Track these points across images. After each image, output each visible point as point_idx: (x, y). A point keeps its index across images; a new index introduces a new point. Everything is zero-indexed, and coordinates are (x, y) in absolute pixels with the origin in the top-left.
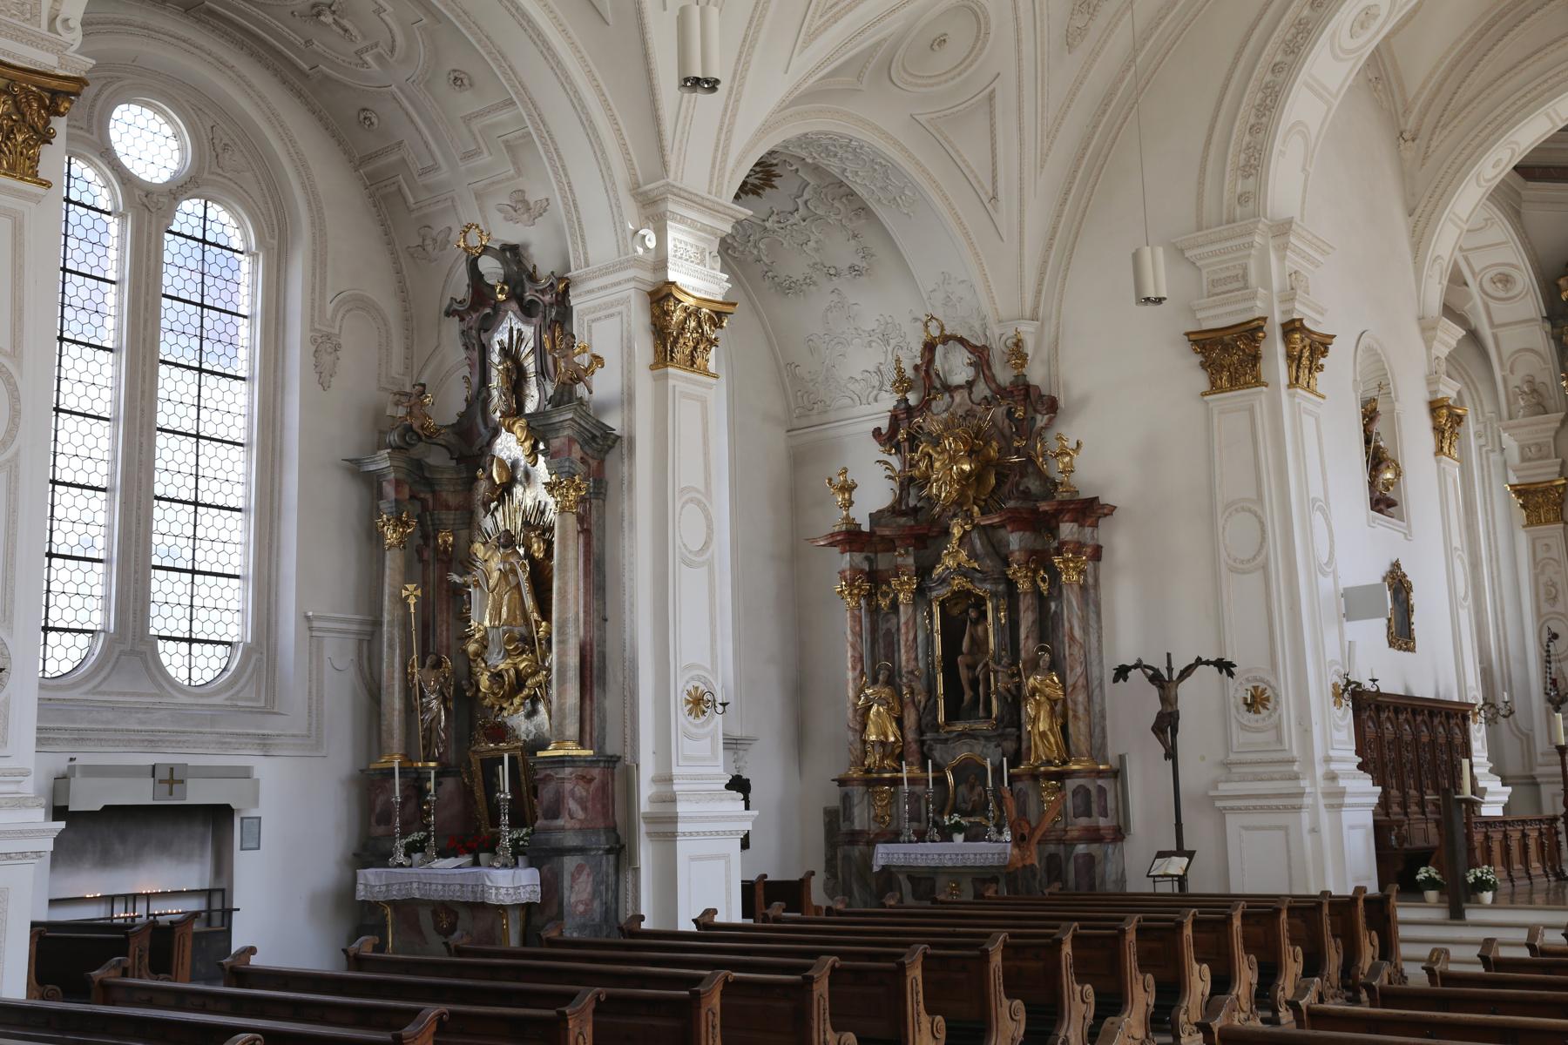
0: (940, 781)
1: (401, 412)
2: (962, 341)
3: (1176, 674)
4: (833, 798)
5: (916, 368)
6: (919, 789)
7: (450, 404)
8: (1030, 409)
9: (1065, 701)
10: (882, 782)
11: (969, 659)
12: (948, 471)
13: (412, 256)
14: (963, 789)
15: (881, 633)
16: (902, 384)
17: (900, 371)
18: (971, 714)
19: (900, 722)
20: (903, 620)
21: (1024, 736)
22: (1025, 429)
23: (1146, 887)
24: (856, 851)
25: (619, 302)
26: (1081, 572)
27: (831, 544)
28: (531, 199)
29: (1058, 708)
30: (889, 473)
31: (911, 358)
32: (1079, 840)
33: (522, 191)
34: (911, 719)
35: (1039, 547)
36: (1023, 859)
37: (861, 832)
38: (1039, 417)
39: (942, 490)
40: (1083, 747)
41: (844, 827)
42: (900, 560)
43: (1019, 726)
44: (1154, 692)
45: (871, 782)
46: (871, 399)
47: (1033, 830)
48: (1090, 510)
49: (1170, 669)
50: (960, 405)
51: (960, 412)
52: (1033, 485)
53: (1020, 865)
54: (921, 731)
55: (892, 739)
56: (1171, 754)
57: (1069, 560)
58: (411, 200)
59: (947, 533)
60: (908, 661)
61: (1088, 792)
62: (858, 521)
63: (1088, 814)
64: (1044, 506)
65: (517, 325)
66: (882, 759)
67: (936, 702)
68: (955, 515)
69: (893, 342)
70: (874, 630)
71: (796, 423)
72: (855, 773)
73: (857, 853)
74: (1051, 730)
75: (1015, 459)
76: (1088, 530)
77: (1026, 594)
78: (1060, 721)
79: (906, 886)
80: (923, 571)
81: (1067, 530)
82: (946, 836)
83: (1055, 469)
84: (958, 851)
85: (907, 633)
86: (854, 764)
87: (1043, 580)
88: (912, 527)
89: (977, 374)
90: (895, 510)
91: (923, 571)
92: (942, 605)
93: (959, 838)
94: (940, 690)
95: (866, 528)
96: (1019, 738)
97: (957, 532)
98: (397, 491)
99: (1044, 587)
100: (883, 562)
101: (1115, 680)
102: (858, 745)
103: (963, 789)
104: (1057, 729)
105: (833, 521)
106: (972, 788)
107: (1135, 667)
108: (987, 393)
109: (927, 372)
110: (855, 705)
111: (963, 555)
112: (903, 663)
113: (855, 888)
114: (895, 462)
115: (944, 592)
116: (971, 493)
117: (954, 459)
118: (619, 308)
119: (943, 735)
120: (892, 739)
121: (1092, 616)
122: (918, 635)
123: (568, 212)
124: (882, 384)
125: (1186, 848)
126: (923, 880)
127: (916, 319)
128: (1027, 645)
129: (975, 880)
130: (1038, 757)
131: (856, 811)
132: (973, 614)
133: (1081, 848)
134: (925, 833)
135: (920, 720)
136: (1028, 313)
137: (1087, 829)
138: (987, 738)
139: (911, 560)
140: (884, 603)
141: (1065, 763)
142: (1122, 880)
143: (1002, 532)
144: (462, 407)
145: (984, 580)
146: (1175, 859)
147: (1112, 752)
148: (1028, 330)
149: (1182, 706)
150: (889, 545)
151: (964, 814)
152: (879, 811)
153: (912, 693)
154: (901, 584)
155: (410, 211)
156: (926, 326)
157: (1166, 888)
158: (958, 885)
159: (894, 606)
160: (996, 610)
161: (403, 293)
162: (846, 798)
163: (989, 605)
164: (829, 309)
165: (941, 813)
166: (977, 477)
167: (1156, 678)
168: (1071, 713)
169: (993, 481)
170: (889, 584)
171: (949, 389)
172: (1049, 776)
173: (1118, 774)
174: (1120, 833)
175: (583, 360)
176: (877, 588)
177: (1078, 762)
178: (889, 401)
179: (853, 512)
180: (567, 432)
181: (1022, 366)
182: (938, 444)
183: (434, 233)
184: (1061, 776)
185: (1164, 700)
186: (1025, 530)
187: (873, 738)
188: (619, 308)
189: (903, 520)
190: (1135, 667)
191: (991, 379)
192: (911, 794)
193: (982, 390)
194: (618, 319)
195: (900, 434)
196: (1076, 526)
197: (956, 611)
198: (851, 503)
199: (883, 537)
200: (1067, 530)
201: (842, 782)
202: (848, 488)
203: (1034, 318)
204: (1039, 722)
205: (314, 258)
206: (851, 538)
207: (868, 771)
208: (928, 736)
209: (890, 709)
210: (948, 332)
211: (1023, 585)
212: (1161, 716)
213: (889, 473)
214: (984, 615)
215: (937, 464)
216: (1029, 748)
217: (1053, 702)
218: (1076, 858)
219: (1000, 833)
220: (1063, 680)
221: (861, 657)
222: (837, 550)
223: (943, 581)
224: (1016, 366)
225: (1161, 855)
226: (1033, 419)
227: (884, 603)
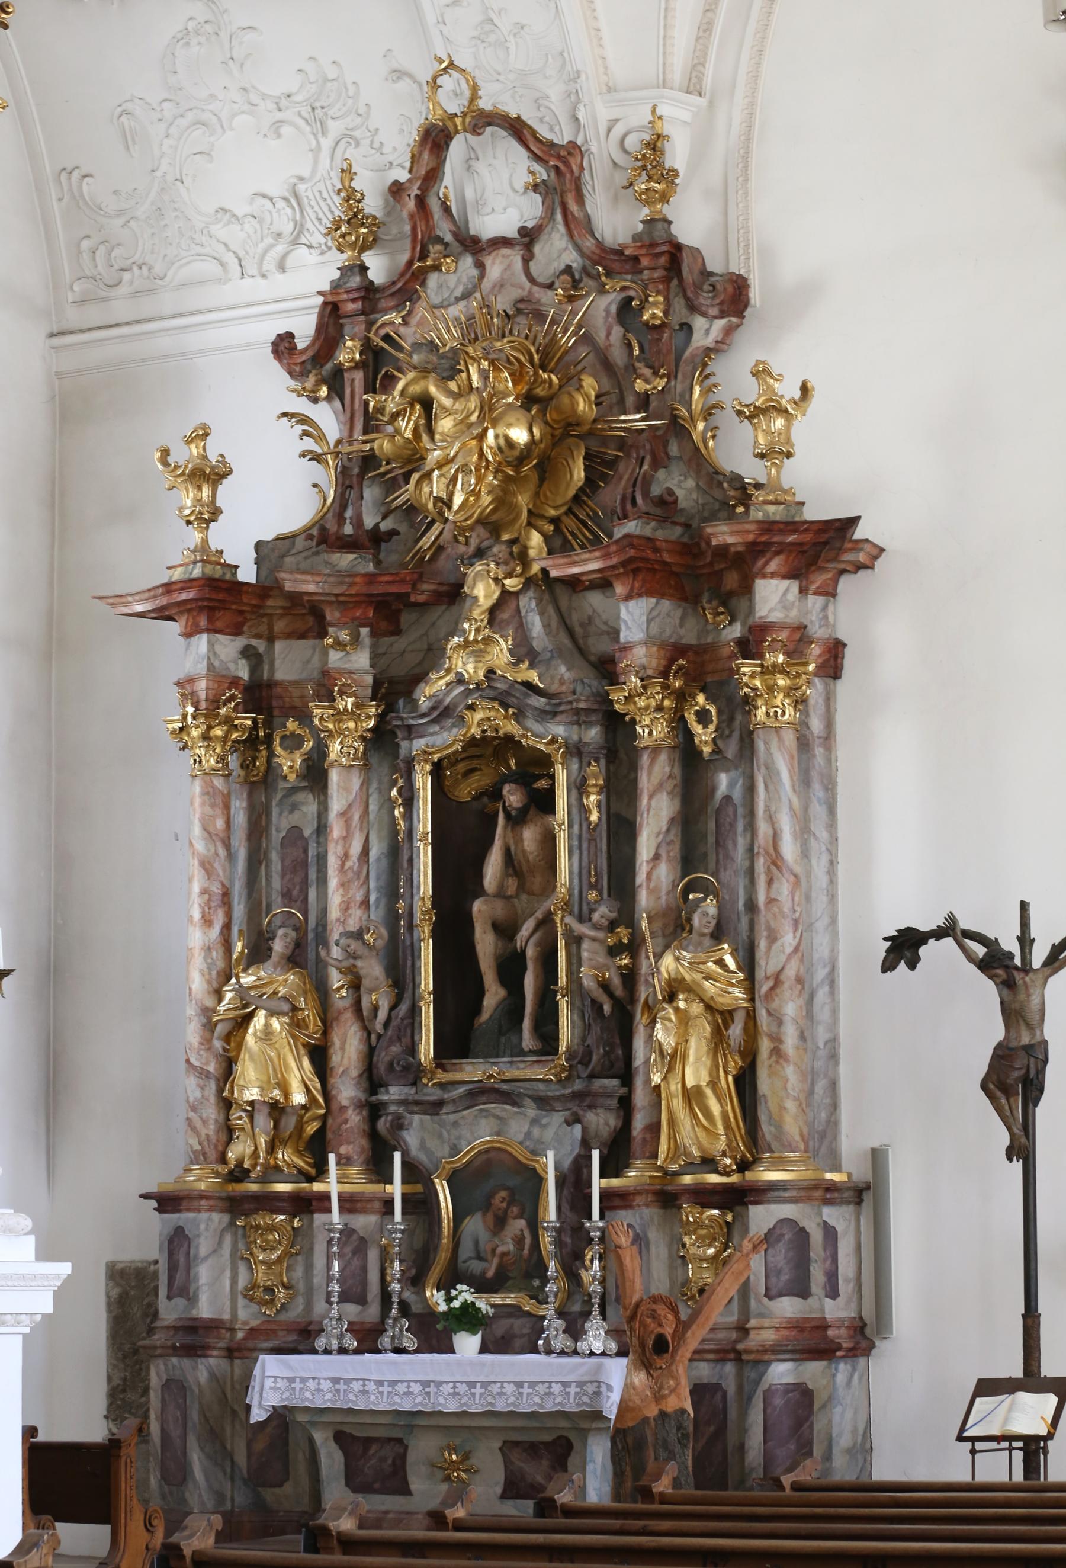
0: (420, 1205)
2: (517, 129)
3: (1038, 958)
4: (143, 1238)
5: (396, 190)
6: (365, 1222)
8: (679, 304)
9: (751, 1016)
10: (268, 1202)
11: (499, 909)
12: (467, 444)
14: (475, 1225)
15: (276, 837)
16: (355, 228)
17: (351, 197)
18: (503, 1037)
19: (319, 1056)
20: (336, 804)
21: (640, 1098)
22: (664, 349)
23: (953, 1467)
24: (200, 1373)
26: (800, 702)
27: (163, 614)
29: (736, 1031)
30: (309, 444)
31: (386, 156)
32: (777, 1351)
34: (348, 1049)
35: (689, 637)
36: (658, 1398)
37: (213, 1326)
38: (699, 323)
39: (455, 486)
40: (792, 1127)
41: (170, 1311)
42: (335, 657)
43: (627, 1076)
44: (986, 992)
45: (242, 1201)
46: (270, 263)
47: (683, 1327)
48: (827, 549)
49: (1025, 941)
50: (500, 285)
51: (503, 303)
52: (680, 484)
53: (652, 1412)
54: (372, 1081)
55: (299, 1098)
56: (1021, 1149)
57: (776, 669)
59: (454, 594)
60: (346, 908)
61: (802, 1235)
62: (229, 558)
63: (803, 1291)
64: (724, 534)
66: (271, 1149)
67: (414, 1011)
68: (480, 554)
69: (335, 128)
70: (258, 829)
71: (73, 317)
72: (201, 1179)
73: (203, 1376)
74: (714, 1084)
75: (635, 420)
76: (815, 602)
77: (656, 750)
78: (735, 1063)
79: (331, 1460)
80: (392, 690)
81: (774, 597)
82: (434, 1334)
83: (736, 451)
84: (465, 1375)
85: (346, 838)
86: (198, 1157)
87: (703, 717)
88: (375, 571)
89: (549, 214)
90: (323, 536)
91: (392, 690)
92: (437, 771)
93: (468, 1343)
94: (427, 981)
95: (247, 574)
96: (626, 1105)
97: (483, 592)
99: (704, 736)
100: (290, 661)
101: (888, 966)
102: (211, 1112)
103: (475, 1225)
104: (727, 1082)
105: (168, 551)
106: (500, 1223)
107: (939, 934)
108: (572, 258)
109: (421, 202)
110: (207, 1012)
111: (501, 653)
112: (334, 912)
113: (196, 1460)
114: (328, 418)
115: (445, 740)
116: (523, 500)
117: (489, 412)
119: (433, 1094)
120: (299, 1098)
121: (818, 811)
122: (363, 839)
124: (300, 229)
125: (1050, 1367)
126: (376, 1448)
127: (399, 74)
128: (655, 875)
129: (508, 1447)
130: (676, 1151)
131: (204, 1273)
132: (513, 797)
133: (781, 1372)
134: (379, 1330)
135: (370, 1053)
136: (677, 75)
137: (798, 1326)
138: (543, 1103)
139: (362, 659)
140: (289, 763)
141: (743, 1166)
142: (864, 1448)
143: (595, 600)
145: (549, 715)
146: (1023, 1397)
147: (853, 1144)
148: (678, 116)
149: (1052, 1031)
150: (310, 619)
151: (482, 1286)
152: (261, 1275)
153: (356, 986)
154: (339, 716)
156: (434, 84)
157: (998, 1468)
158: (466, 1457)
159: (316, 774)
160: (579, 787)
162: (177, 1242)
163: (561, 775)
164: (183, 37)
165: (416, 1280)
166: (537, 465)
167: (994, 962)
168: (765, 1046)
169: (579, 474)
170: (304, 717)
171: (474, 246)
172: (704, 1196)
173: (865, 1194)
174: (862, 1338)
176: (268, 724)
177: (779, 1164)
178: (317, 271)
179: (219, 536)
181: (665, 198)
182: (452, 373)
184: (737, 1198)
185: (1014, 1014)
186: (661, 595)
187: (252, 1094)
189: (345, 560)
190: (939, 934)
191: (578, 226)
192: (347, 1232)
193: (557, 251)
195: (345, 352)
196: (794, 586)
197: (465, 792)
198: (216, 513)
199: (295, 598)
200: (774, 597)
201: (167, 1202)
202: (210, 475)
203: (693, 86)
204: (680, 1062)
206: (213, 599)
207: (239, 1174)
208: (394, 1094)
209: (297, 1024)
210: (485, 104)
211: (651, 729)
212: (1002, 1055)
213: (309, 444)
214: (544, 802)
215: (445, 425)
216: (654, 1128)
217: (721, 1017)
218: (768, 1394)
219: (575, 1331)
220: (749, 964)
221: (226, 895)
222: (174, 628)
223: (442, 713)
224: (647, 198)
225: (987, 1388)
226: (687, 328)
227: (289, 763)
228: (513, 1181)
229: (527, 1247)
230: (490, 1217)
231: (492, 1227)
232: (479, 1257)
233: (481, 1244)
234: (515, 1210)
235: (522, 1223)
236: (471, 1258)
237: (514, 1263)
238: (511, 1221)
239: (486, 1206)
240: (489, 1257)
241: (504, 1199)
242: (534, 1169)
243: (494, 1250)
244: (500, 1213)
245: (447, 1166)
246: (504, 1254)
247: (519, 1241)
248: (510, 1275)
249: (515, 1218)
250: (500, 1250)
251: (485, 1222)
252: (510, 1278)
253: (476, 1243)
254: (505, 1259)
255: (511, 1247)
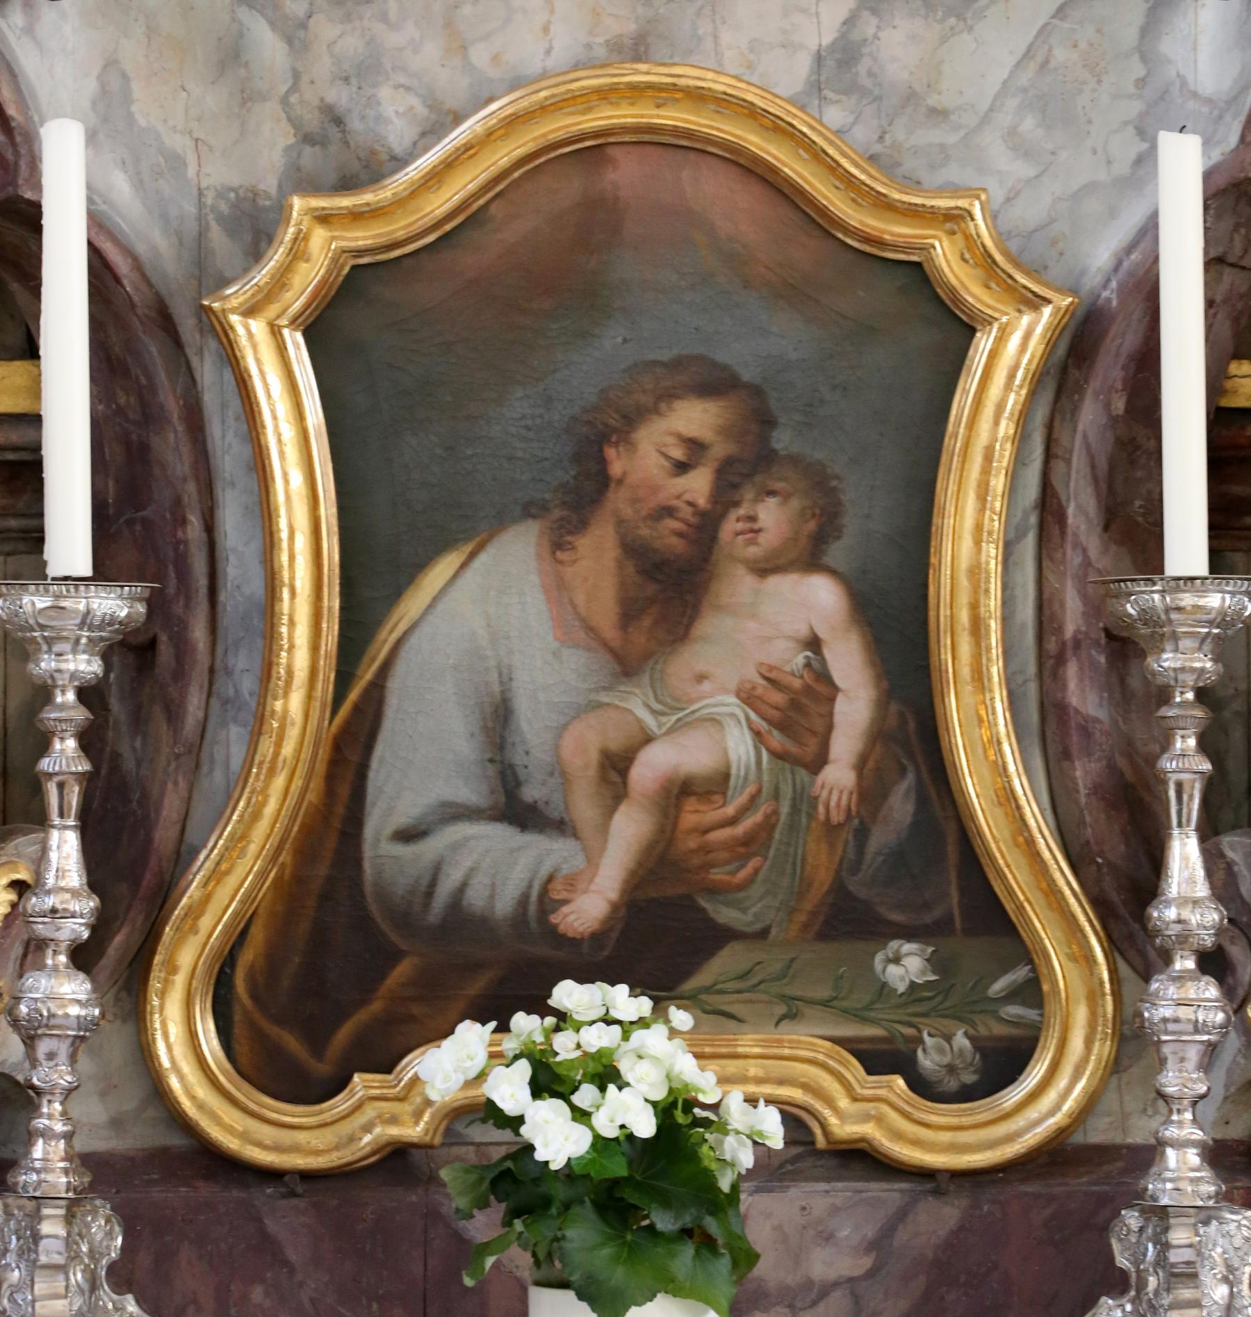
103: (493, 611)
106: (669, 590)
228: (763, 341)
229: (846, 743)
230: (597, 558)
231: (606, 614)
232: (516, 811)
233: (532, 728)
234: (773, 518)
235: (818, 599)
236: (455, 813)
237: (751, 844)
238: (737, 585)
239: (578, 490)
240: (584, 809)
241: (695, 447)
242: (917, 274)
243: (615, 767)
244: (668, 537)
245: (319, 236)
246: (680, 791)
247: (795, 714)
248: (725, 915)
249: (764, 569)
250: (655, 764)
251: (558, 589)
252: (723, 936)
253: (498, 720)
254: (693, 815)
255: (739, 747)
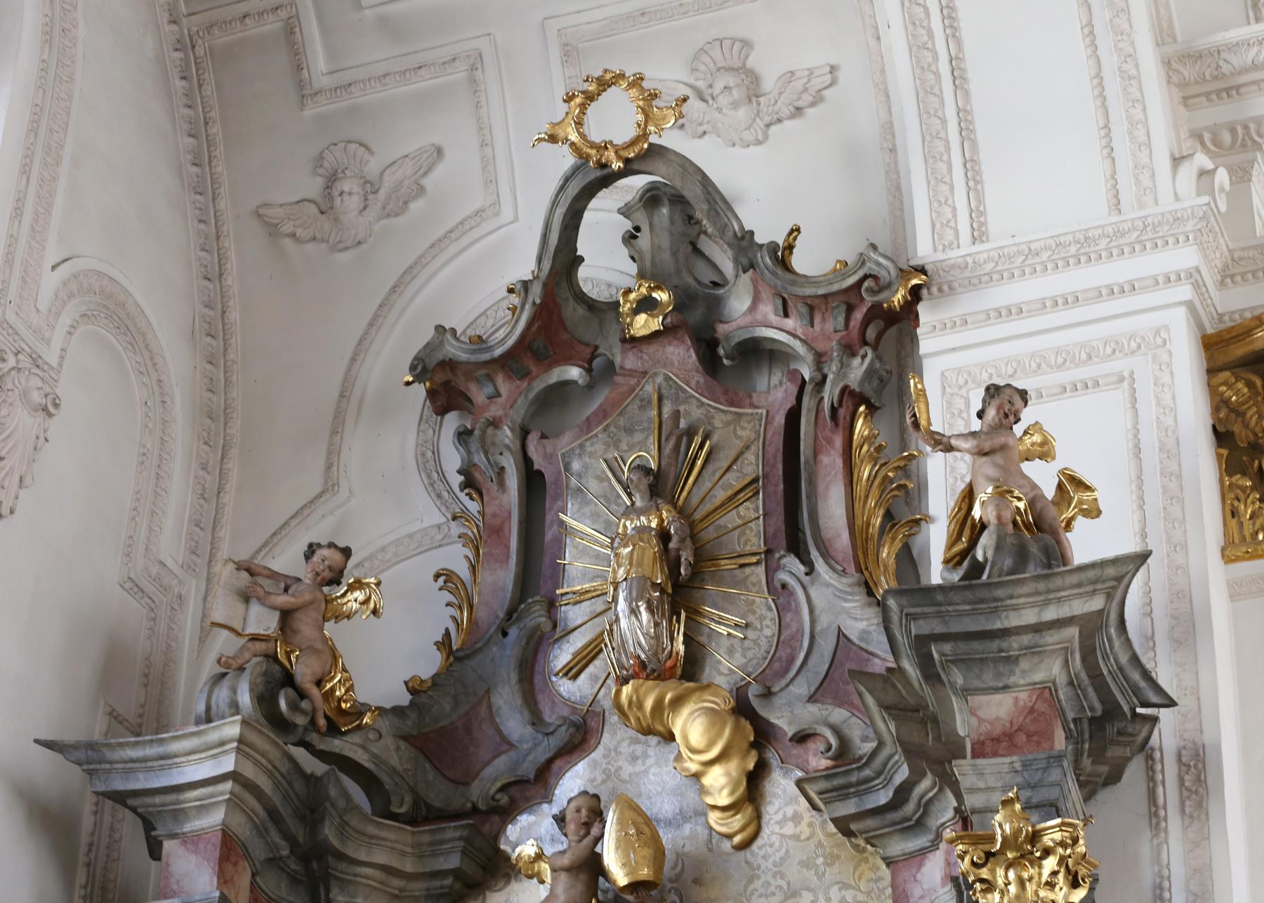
1: (262, 621)
7: (386, 651)
13: (272, 230)
25: (1117, 348)
28: (770, 69)
33: (747, 44)
58: (319, 62)
65: (697, 407)
98: (224, 879)
118: (1120, 365)
123: (926, 91)
144: (429, 664)
155: (304, 92)
161: (214, 330)
175: (1044, 476)
180: (1052, 670)
183: (373, 166)
188: (1120, 365)
194: (1119, 396)
205: (33, 130)
